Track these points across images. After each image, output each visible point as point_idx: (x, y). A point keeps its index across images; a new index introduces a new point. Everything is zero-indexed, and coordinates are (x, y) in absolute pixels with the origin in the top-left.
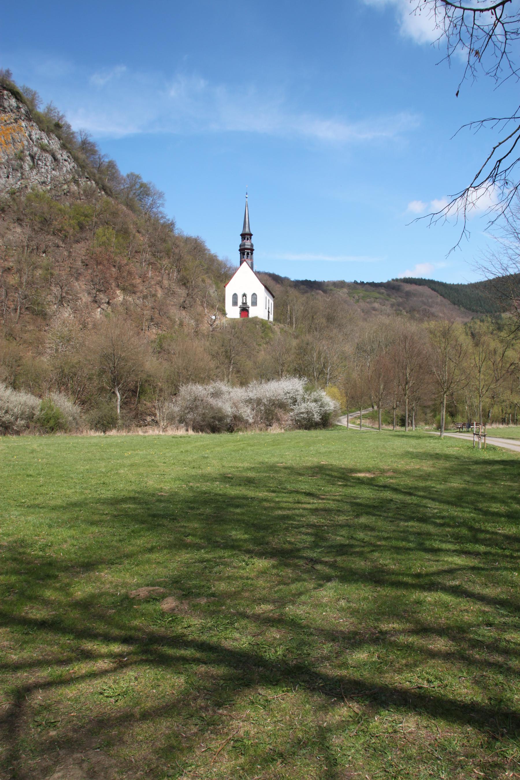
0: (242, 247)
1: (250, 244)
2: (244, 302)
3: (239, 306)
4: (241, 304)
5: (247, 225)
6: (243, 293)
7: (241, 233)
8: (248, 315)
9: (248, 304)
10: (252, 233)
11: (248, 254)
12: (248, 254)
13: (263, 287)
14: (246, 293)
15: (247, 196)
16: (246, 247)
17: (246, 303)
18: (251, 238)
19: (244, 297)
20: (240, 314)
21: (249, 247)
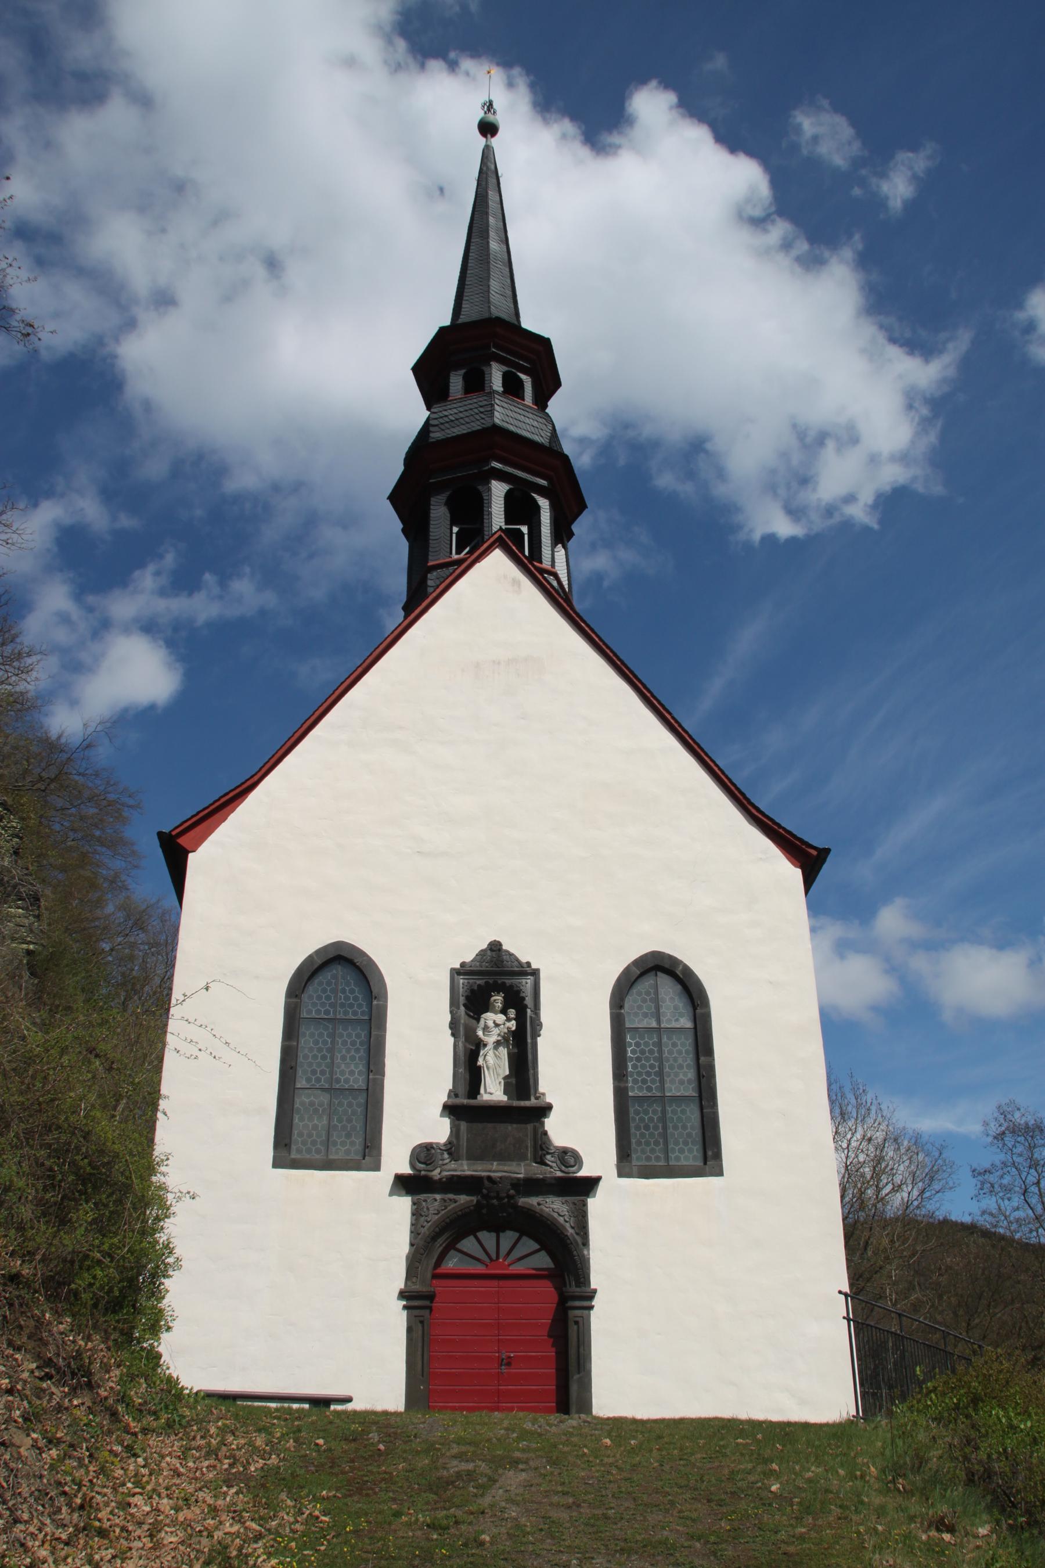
4: (440, 1131)
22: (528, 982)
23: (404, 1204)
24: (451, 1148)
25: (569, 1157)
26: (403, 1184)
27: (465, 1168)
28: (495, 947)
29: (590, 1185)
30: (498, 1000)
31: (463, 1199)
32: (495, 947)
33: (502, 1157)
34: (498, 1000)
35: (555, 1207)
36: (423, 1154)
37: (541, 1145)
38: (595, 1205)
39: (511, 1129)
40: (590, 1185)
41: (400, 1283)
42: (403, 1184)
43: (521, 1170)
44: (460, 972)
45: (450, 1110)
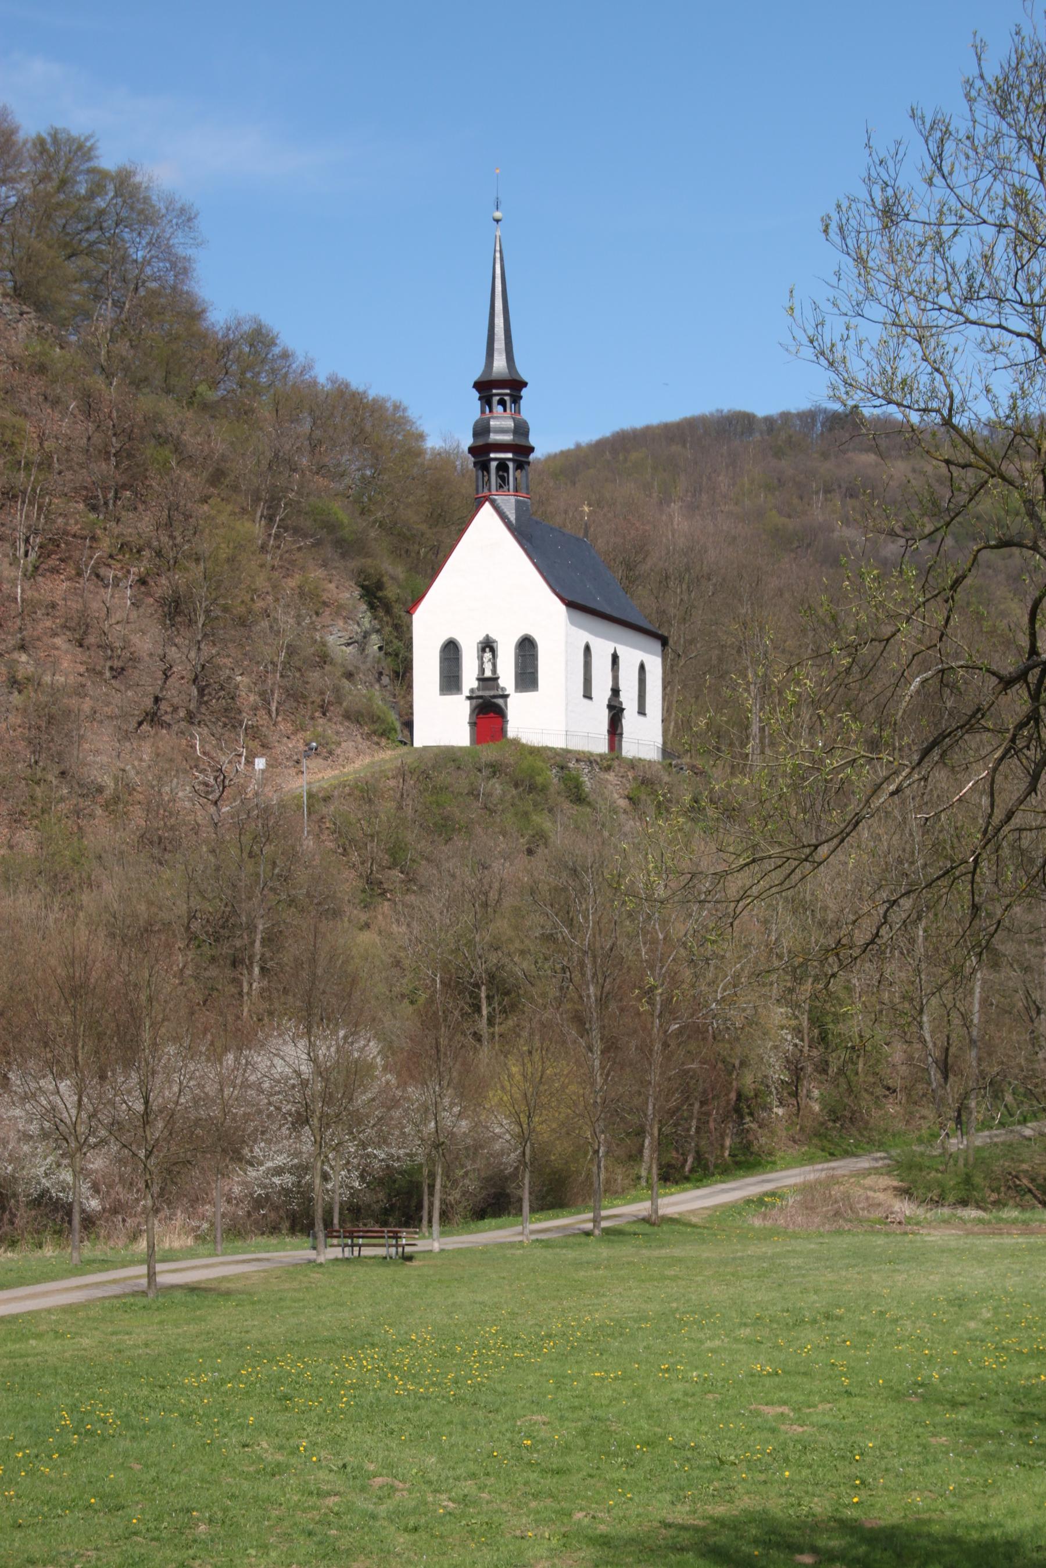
0: (480, 442)
1: (510, 424)
2: (488, 674)
3: (466, 692)
4: (475, 684)
5: (500, 344)
6: (481, 637)
7: (476, 374)
8: (502, 731)
9: (502, 682)
10: (524, 376)
11: (502, 466)
12: (502, 466)
13: (562, 608)
14: (493, 636)
15: (498, 215)
16: (495, 437)
17: (495, 679)
18: (516, 399)
19: (488, 655)
20: (473, 724)
21: (508, 438)
22: (495, 645)
23: (468, 702)
24: (478, 689)
25: (503, 689)
26: (469, 698)
27: (480, 693)
28: (487, 636)
29: (507, 696)
30: (487, 650)
31: (480, 701)
32: (487, 636)
33: (489, 689)
34: (487, 650)
35: (500, 701)
36: (472, 691)
37: (498, 685)
38: (509, 700)
39: (491, 683)
40: (507, 696)
41: (467, 720)
42: (469, 698)
43: (492, 693)
44: (481, 643)
45: (479, 679)
